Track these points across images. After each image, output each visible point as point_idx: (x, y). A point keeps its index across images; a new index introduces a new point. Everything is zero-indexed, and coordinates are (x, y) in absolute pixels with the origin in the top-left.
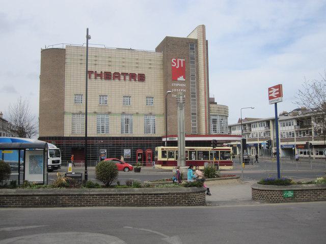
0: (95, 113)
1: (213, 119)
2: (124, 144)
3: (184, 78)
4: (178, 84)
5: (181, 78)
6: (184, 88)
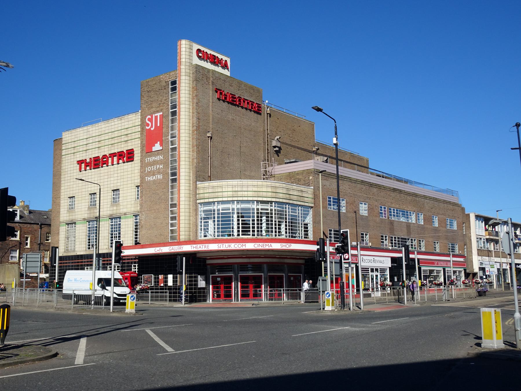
0: (84, 219)
3: (161, 145)
4: (154, 158)
5: (157, 147)
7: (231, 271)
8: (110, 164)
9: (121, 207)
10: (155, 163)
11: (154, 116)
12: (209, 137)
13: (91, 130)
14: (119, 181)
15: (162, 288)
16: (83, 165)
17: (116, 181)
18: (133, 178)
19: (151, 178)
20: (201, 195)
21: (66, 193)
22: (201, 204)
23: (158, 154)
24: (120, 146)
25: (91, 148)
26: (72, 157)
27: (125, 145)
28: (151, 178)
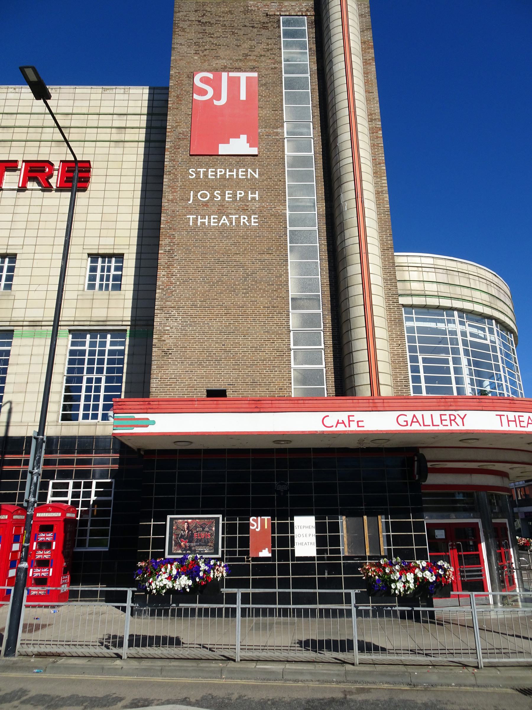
3: (251, 143)
4: (220, 172)
5: (239, 145)
6: (251, 185)
10: (223, 184)
11: (224, 75)
15: (263, 567)
20: (416, 286)
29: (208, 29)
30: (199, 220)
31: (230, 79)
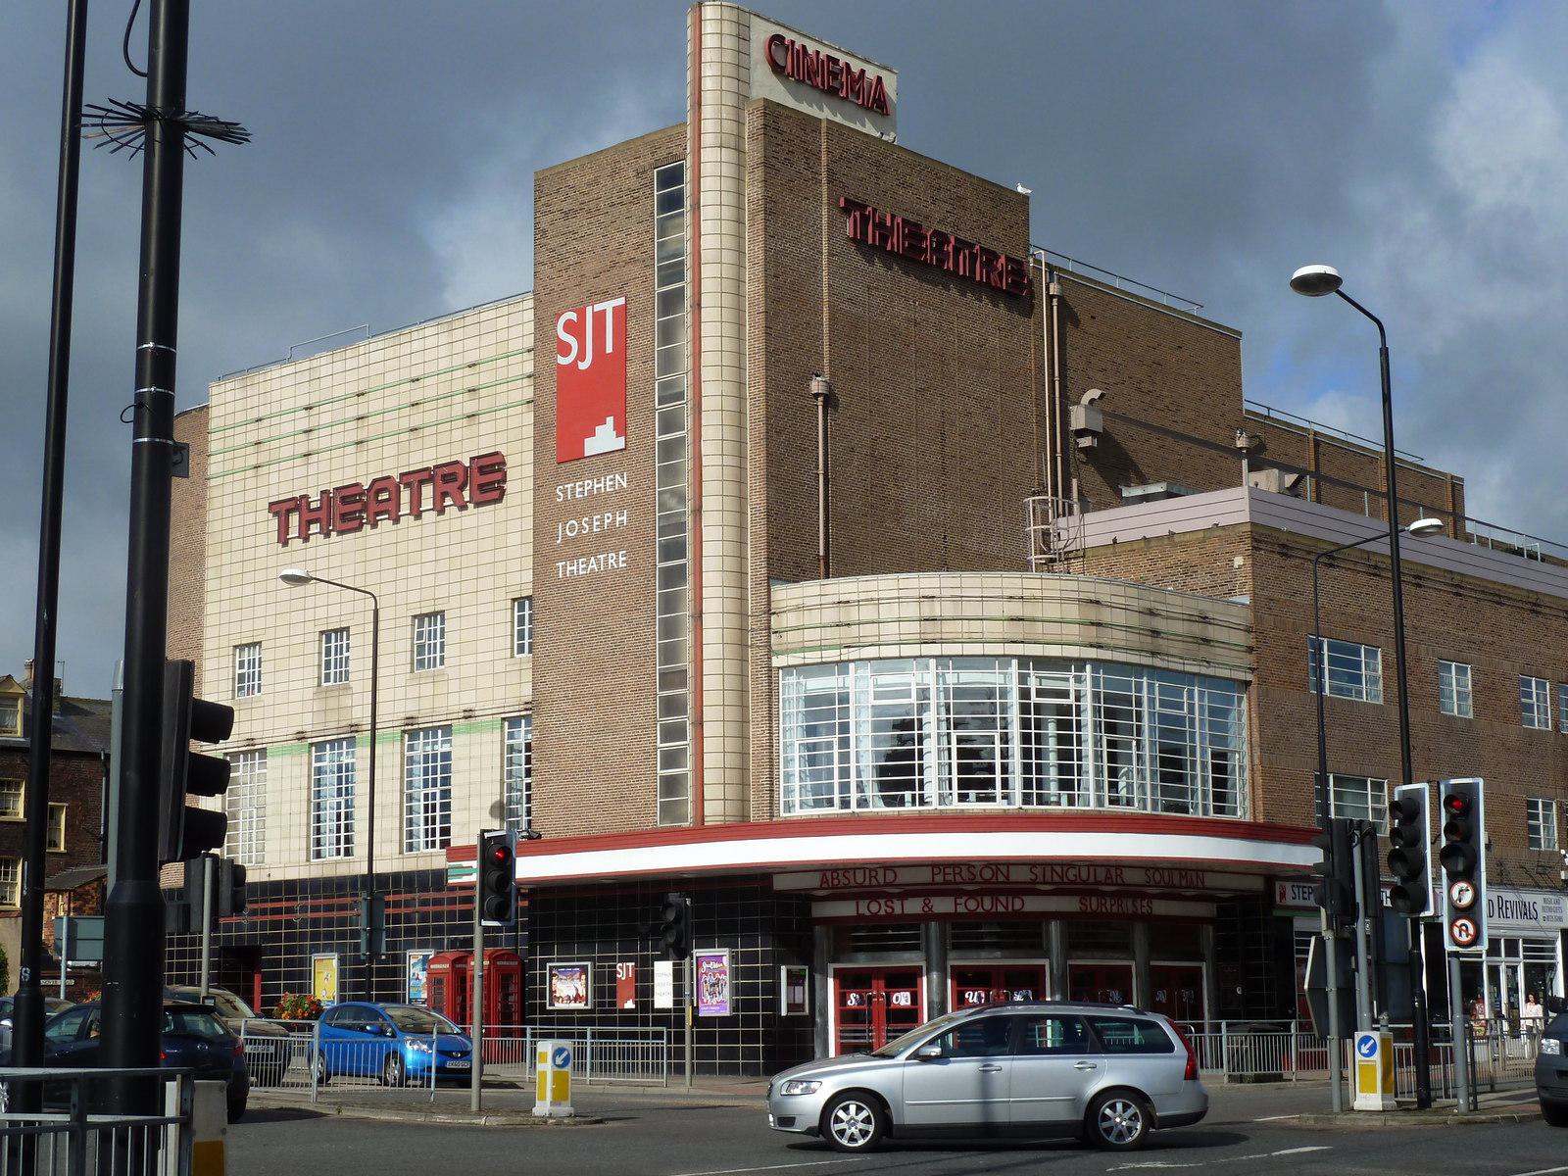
0: (301, 736)
1: (810, 701)
2: (409, 918)
3: (621, 429)
5: (604, 439)
7: (916, 948)
8: (405, 509)
9: (454, 686)
10: (595, 503)
11: (589, 310)
12: (816, 396)
13: (324, 371)
14: (442, 578)
15: (628, 1018)
16: (294, 519)
17: (428, 581)
18: (500, 568)
19: (578, 568)
20: (792, 637)
21: (224, 630)
22: (788, 669)
23: (609, 469)
24: (444, 438)
25: (325, 443)
26: (251, 483)
27: (467, 432)
28: (578, 568)
29: (573, 223)
30: (569, 568)
31: (595, 314)
